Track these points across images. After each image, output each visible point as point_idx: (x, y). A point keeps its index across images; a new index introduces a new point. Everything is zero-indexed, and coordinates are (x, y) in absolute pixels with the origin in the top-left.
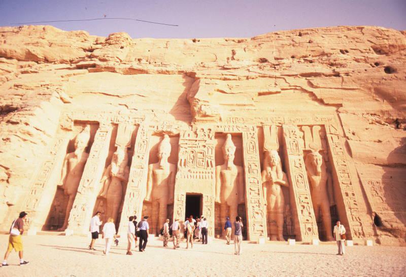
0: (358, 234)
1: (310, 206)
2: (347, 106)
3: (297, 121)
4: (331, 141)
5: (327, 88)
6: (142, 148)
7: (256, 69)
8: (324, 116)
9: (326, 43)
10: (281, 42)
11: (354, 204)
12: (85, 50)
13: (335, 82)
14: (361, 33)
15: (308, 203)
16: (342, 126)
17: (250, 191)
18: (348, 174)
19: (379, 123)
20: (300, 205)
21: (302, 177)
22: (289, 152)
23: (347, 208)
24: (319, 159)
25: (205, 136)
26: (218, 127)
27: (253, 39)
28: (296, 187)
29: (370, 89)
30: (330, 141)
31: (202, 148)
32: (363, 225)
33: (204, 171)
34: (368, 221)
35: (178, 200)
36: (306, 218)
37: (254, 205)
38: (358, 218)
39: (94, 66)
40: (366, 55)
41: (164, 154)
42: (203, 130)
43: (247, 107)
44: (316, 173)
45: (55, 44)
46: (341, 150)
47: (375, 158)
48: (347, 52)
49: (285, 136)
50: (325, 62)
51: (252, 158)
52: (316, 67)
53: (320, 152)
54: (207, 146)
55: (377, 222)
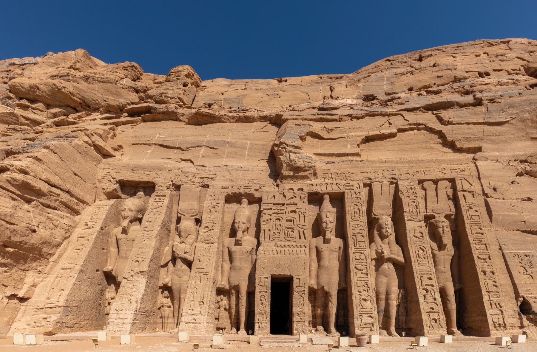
0: (497, 325)
1: (435, 290)
3: (418, 175)
4: (463, 198)
6: (212, 217)
8: (455, 167)
11: (494, 285)
14: (507, 48)
15: (433, 286)
16: (479, 179)
17: (356, 270)
18: (486, 244)
19: (529, 174)
20: (421, 288)
21: (424, 251)
22: (406, 216)
23: (484, 291)
25: (296, 197)
26: (313, 185)
28: (417, 264)
30: (462, 202)
31: (293, 214)
32: (504, 313)
33: (295, 244)
35: (261, 286)
36: (429, 305)
37: (361, 289)
38: (499, 304)
41: (241, 223)
42: (292, 189)
43: (350, 158)
45: (94, 78)
46: (477, 213)
47: (525, 222)
48: (487, 74)
49: (401, 195)
50: (456, 90)
51: (357, 224)
54: (297, 211)
55: (525, 308)
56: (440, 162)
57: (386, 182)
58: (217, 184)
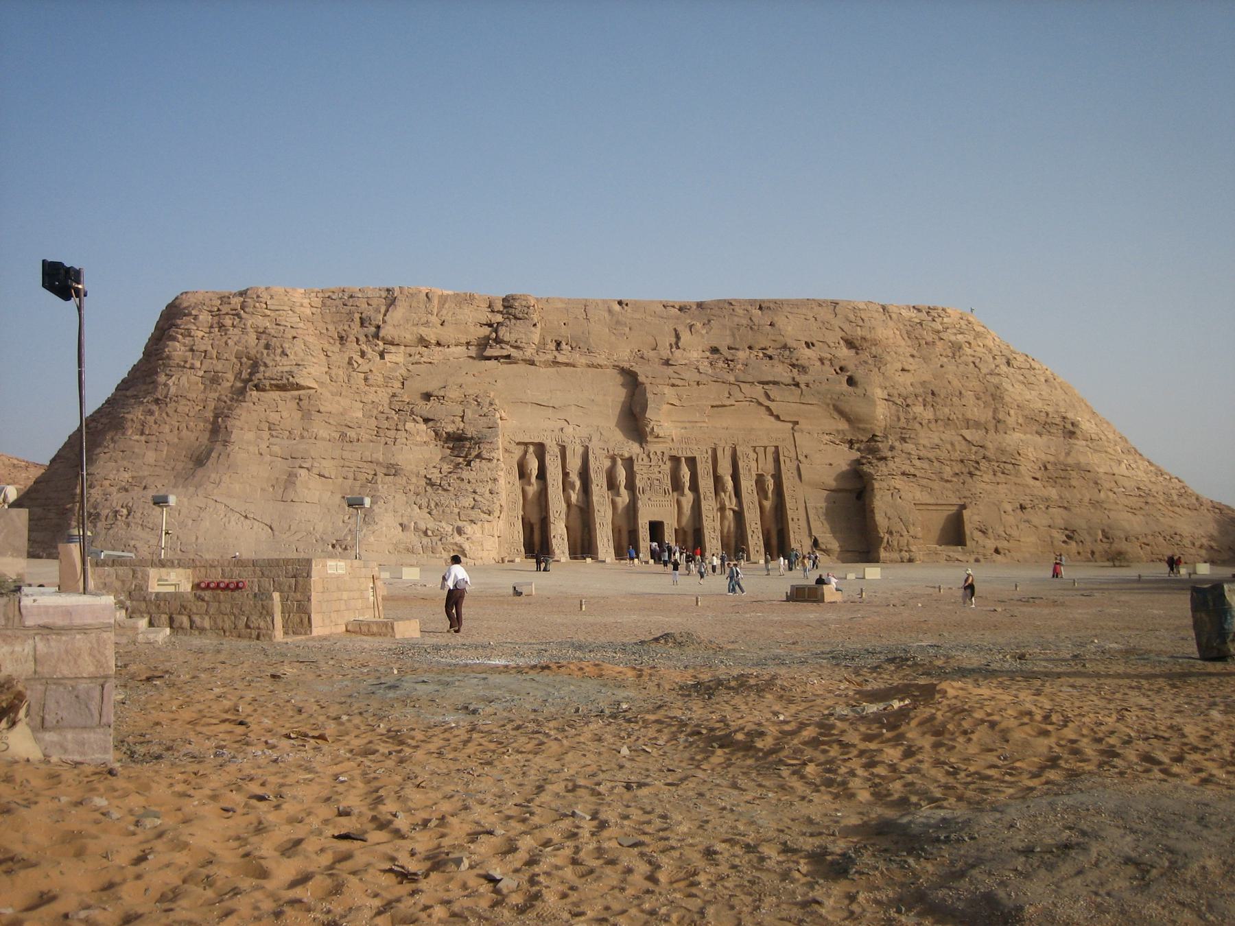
2: (803, 424)
5: (785, 402)
7: (705, 366)
9: (790, 328)
10: (736, 319)
12: (482, 325)
13: (792, 395)
24: (770, 484)
27: (700, 305)
29: (828, 405)
34: (808, 543)
36: (755, 541)
39: (508, 357)
40: (833, 351)
44: (766, 498)
52: (775, 370)
53: (773, 476)
56: (768, 430)
57: (727, 448)
58: (595, 446)
